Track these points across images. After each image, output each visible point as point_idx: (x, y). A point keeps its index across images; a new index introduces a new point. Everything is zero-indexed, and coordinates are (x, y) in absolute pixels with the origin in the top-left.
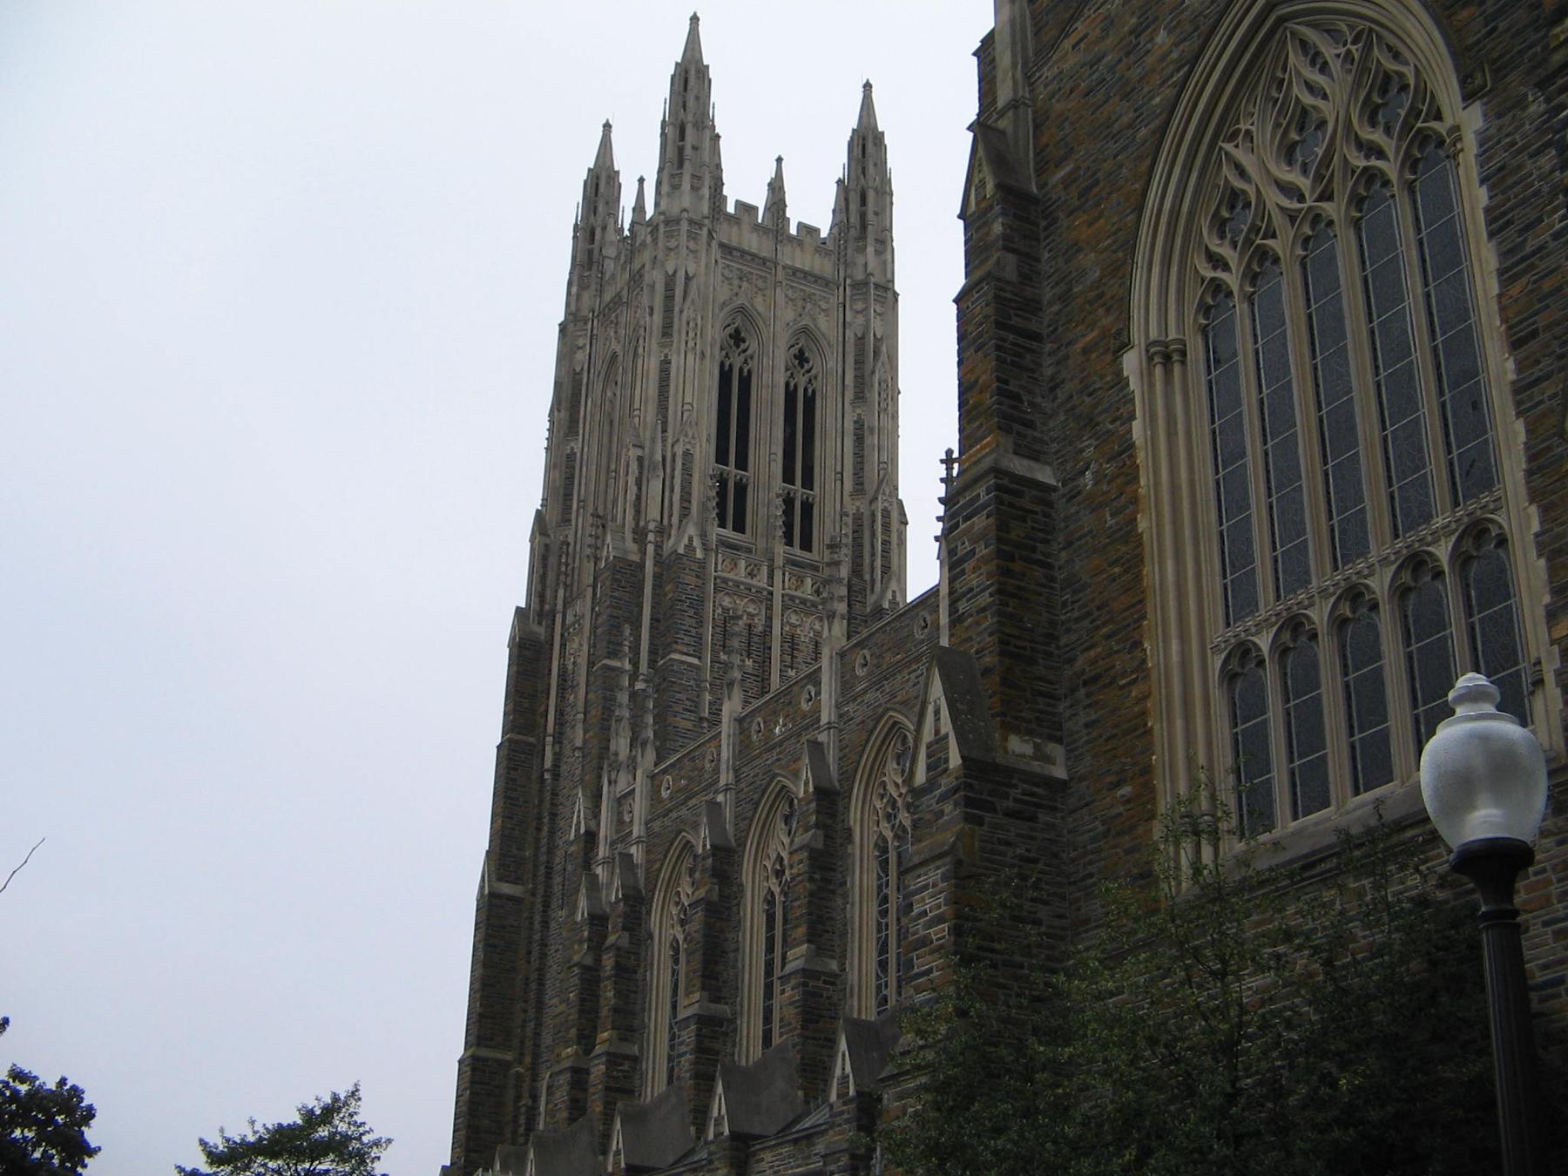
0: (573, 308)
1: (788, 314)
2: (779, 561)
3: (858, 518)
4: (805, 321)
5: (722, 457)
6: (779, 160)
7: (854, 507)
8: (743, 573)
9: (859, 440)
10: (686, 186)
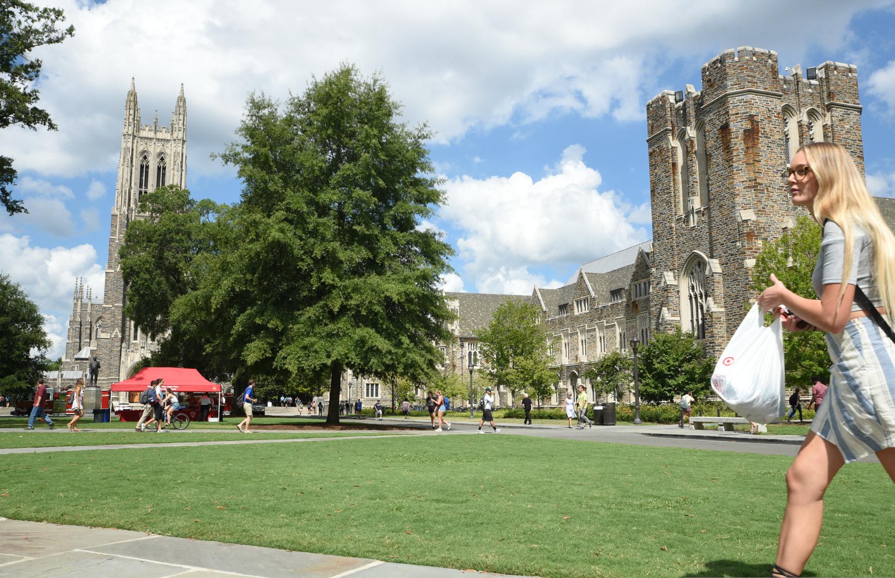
1: (158, 150)
4: (163, 151)
5: (141, 186)
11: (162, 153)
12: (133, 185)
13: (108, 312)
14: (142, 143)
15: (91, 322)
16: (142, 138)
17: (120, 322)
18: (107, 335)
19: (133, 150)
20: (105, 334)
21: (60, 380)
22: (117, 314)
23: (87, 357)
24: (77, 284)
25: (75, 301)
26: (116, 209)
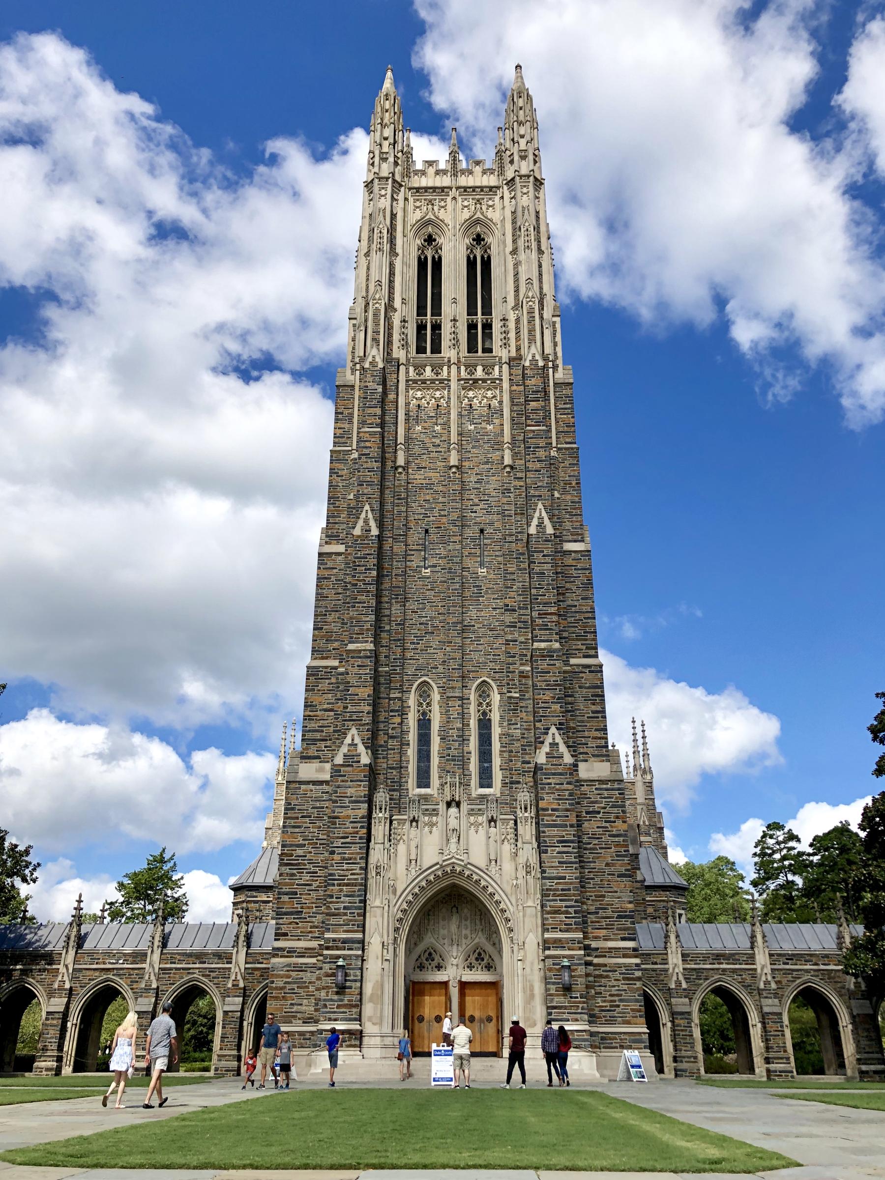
1: (466, 214)
3: (518, 321)
4: (478, 215)
9: (516, 275)
10: (377, 160)
11: (478, 222)
12: (397, 304)
13: (324, 685)
14: (418, 204)
16: (418, 189)
17: (370, 708)
18: (321, 770)
20: (315, 765)
21: (156, 956)
22: (353, 680)
26: (349, 372)
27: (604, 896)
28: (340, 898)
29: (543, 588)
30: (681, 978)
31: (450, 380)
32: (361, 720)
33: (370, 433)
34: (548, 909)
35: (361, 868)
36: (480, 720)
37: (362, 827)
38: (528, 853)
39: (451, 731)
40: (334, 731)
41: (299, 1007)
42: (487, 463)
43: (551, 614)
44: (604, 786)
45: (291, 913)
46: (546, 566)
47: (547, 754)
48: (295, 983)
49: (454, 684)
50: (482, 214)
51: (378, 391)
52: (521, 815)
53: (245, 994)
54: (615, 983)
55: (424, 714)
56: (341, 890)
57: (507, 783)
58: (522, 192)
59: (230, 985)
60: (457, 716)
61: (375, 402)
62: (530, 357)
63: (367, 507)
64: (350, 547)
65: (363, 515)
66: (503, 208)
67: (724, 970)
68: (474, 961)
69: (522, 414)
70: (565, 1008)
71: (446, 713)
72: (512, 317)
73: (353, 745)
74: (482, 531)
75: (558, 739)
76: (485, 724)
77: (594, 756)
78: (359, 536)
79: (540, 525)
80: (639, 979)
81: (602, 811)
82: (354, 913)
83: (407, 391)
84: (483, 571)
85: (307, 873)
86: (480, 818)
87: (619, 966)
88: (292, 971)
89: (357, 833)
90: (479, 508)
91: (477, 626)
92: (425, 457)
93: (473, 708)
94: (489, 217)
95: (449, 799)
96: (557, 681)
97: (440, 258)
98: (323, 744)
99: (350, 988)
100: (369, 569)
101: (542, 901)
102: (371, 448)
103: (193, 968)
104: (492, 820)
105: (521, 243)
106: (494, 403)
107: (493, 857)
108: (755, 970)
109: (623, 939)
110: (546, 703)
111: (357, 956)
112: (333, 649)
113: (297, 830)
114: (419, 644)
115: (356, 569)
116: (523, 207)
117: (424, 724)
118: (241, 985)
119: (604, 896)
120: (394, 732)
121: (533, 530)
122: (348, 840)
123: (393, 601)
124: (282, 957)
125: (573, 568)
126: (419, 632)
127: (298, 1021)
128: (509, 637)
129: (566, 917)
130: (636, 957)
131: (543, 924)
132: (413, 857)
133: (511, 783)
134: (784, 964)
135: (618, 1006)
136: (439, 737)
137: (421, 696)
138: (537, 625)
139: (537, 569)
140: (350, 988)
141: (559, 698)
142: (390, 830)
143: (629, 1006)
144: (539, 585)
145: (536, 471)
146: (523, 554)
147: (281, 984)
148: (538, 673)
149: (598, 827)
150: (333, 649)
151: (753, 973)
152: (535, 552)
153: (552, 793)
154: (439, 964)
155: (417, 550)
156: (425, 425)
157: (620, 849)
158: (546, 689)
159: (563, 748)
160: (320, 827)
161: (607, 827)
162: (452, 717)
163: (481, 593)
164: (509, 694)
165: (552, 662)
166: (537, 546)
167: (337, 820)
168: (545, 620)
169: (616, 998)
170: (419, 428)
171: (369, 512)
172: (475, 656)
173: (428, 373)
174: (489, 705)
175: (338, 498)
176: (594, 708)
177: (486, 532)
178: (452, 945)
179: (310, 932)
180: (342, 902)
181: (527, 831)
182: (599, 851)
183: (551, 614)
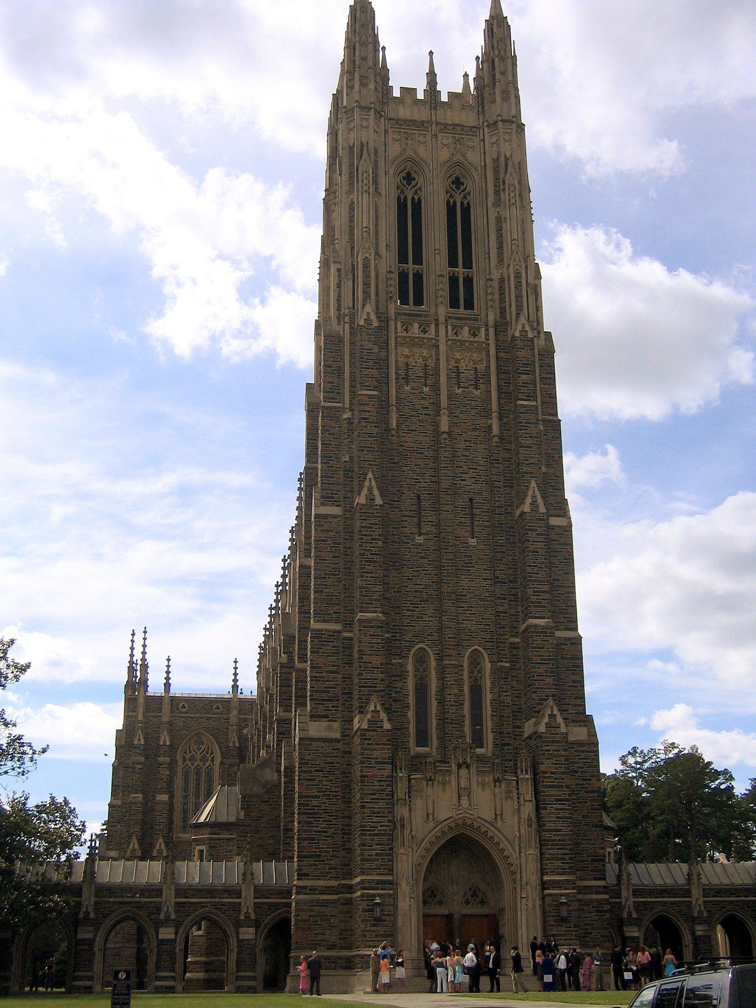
0: (328, 187)
1: (444, 154)
2: (442, 319)
3: (502, 280)
4: (458, 157)
5: (403, 258)
6: (431, 53)
7: (499, 274)
8: (416, 331)
9: (499, 230)
10: (357, 86)
15: (171, 746)
18: (329, 729)
19: (376, 151)
20: (324, 724)
22: (367, 651)
23: (233, 819)
24: (132, 648)
25: (130, 692)
27: (581, 843)
28: (372, 846)
29: (537, 566)
30: (632, 909)
31: (438, 341)
32: (376, 687)
33: (369, 396)
34: (548, 856)
35: (389, 821)
36: (471, 686)
37: (388, 785)
38: (528, 809)
39: (449, 697)
40: (343, 694)
41: (322, 936)
42: (475, 430)
43: (543, 592)
44: (584, 749)
45: (312, 856)
46: (540, 545)
47: (546, 724)
48: (318, 916)
49: (452, 652)
50: (464, 155)
51: (374, 351)
52: (522, 777)
53: (257, 924)
54: (588, 915)
55: (421, 678)
56: (372, 840)
57: (498, 745)
58: (504, 139)
59: (242, 917)
60: (454, 683)
61: (371, 363)
62: (519, 328)
63: (370, 475)
64: (348, 511)
65: (367, 484)
66: (485, 153)
67: (666, 903)
68: (470, 899)
69: (510, 383)
70: (562, 935)
71: (442, 678)
72: (495, 275)
73: (375, 711)
74: (471, 500)
75: (556, 711)
76: (476, 692)
77: (573, 721)
78: (364, 505)
79: (534, 503)
80: (607, 911)
81: (581, 770)
82: (384, 859)
83: (396, 349)
84: (473, 542)
85: (323, 821)
86: (487, 779)
87: (591, 901)
88: (316, 906)
89: (383, 790)
90: (468, 476)
91: (469, 596)
92: (415, 419)
93: (466, 674)
94: (470, 160)
95: (461, 761)
96: (550, 656)
97: (420, 200)
98: (329, 705)
99: (385, 921)
100: (375, 539)
101: (541, 850)
102: (369, 412)
103: (206, 902)
104: (497, 781)
105: (504, 196)
106: (481, 367)
107: (499, 812)
108: (691, 902)
109: (595, 879)
110: (541, 676)
111: (390, 896)
112: (334, 613)
113: (311, 783)
114: (414, 611)
115: (363, 539)
116: (505, 156)
117: (422, 690)
118: (253, 916)
119: (581, 843)
120: (395, 695)
121: (527, 508)
122: (376, 796)
123: (391, 568)
124: (305, 894)
125: (556, 542)
126: (415, 600)
127: (322, 948)
128: (501, 609)
129: (562, 863)
130: (606, 893)
131: (542, 869)
132: (431, 811)
133: (504, 745)
134: (714, 896)
135: (591, 933)
136: (436, 701)
137: (417, 662)
138: (532, 602)
139: (531, 548)
140: (385, 921)
141: (552, 672)
142: (409, 787)
143: (599, 933)
144: (533, 563)
145: (528, 447)
146: (513, 528)
147: (305, 917)
148: (533, 647)
149: (577, 784)
150: (334, 613)
151: (689, 905)
152: (530, 530)
153: (550, 759)
154: (440, 900)
155: (410, 516)
156: (414, 385)
157: (594, 804)
158: (541, 663)
159: (559, 719)
160: (332, 781)
161: (584, 785)
162: (449, 683)
163: (472, 563)
164: (500, 664)
165: (546, 638)
166: (531, 524)
167: (366, 779)
168: (539, 597)
169: (589, 927)
170: (407, 388)
171: (373, 480)
172: (466, 624)
173: (415, 329)
174: (479, 672)
175: (332, 457)
176: (573, 677)
177: (475, 501)
178: (452, 884)
179: (330, 873)
180: (373, 850)
181: (527, 791)
182: (578, 805)
183: (543, 592)
